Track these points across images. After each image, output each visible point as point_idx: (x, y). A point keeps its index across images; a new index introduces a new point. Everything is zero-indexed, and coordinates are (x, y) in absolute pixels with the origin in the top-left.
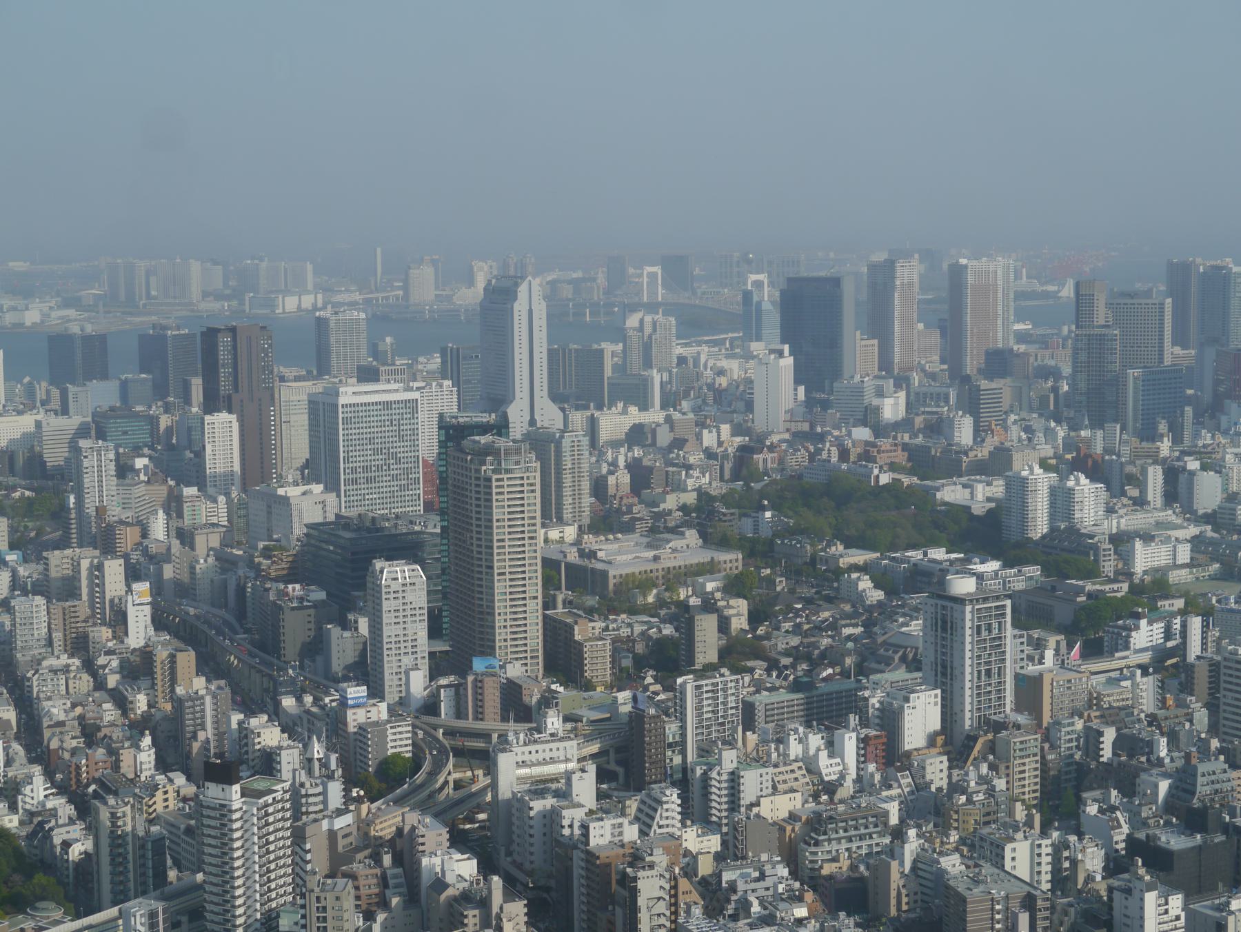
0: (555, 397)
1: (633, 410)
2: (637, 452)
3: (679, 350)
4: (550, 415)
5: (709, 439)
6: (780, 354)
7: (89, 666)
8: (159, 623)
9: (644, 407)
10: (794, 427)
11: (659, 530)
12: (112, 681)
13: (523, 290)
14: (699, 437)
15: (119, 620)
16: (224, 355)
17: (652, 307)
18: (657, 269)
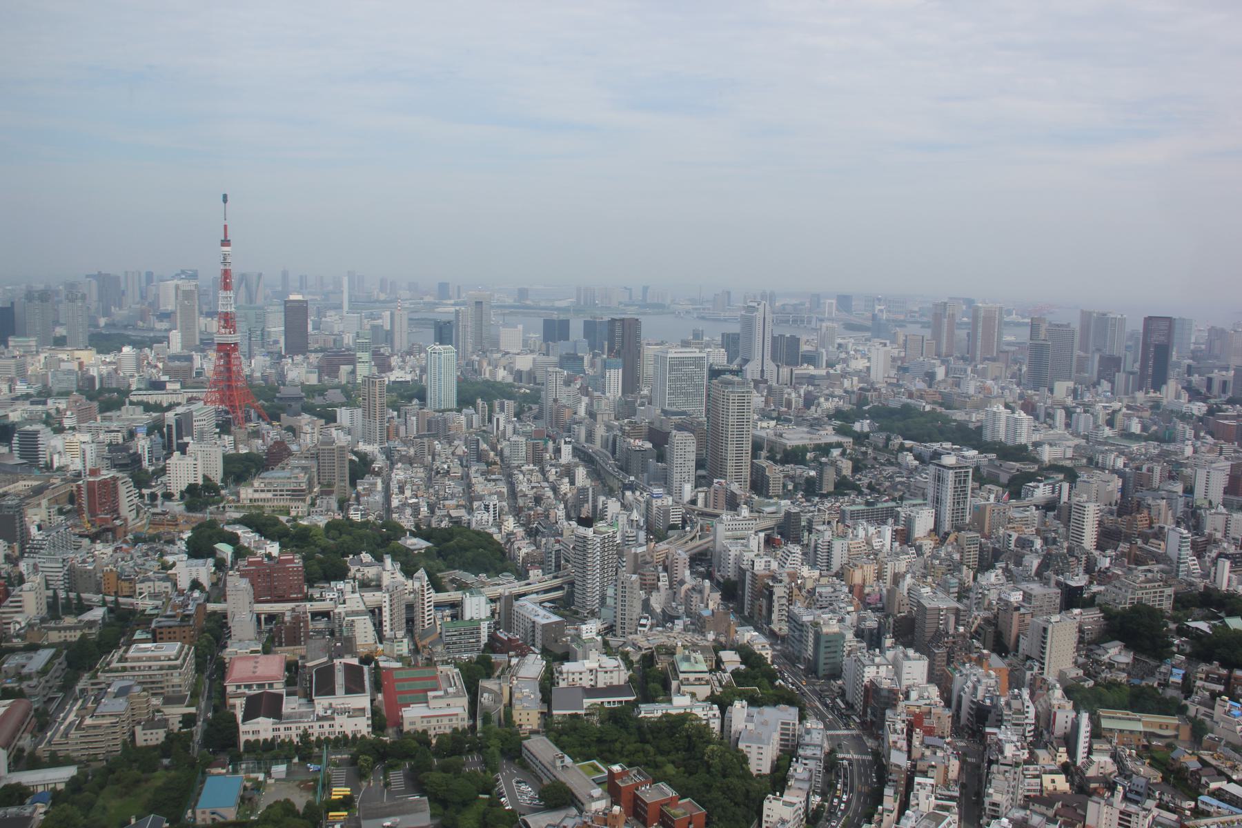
0: (774, 359)
1: (812, 367)
2: (811, 388)
3: (839, 341)
4: (770, 366)
5: (847, 384)
6: (885, 345)
7: (543, 472)
8: (577, 452)
9: (816, 366)
10: (889, 380)
11: (815, 424)
12: (552, 478)
13: (761, 307)
14: (842, 384)
15: (558, 451)
16: (618, 332)
17: (832, 320)
18: (834, 301)
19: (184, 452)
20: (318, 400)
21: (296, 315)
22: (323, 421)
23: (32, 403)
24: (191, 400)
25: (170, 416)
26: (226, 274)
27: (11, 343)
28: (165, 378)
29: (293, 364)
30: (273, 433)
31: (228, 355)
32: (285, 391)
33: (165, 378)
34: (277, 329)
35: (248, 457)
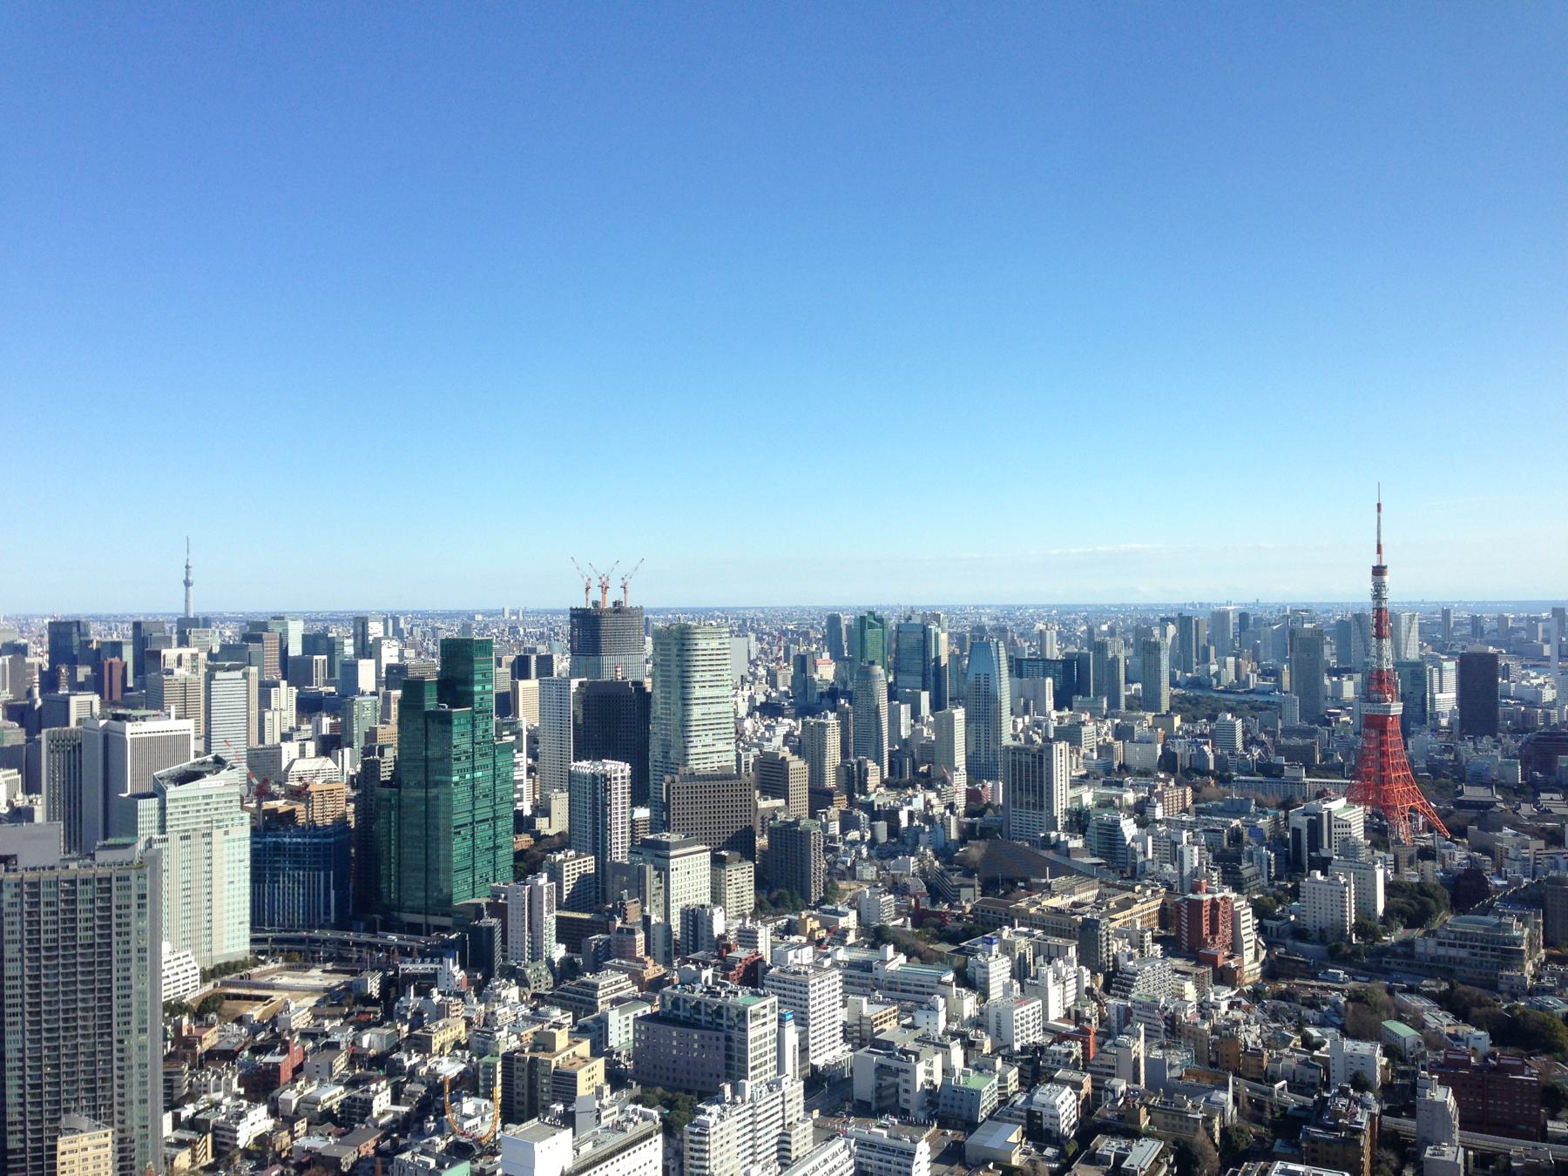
19: (1324, 873)
20: (1526, 809)
21: (1479, 677)
22: (1541, 844)
23: (1105, 784)
24: (1321, 795)
25: (1299, 820)
26: (1379, 611)
27: (1075, 705)
28: (1282, 760)
29: (1475, 749)
30: (1459, 856)
31: (1383, 732)
32: (1472, 793)
33: (1282, 760)
34: (1446, 699)
35: (1421, 889)
